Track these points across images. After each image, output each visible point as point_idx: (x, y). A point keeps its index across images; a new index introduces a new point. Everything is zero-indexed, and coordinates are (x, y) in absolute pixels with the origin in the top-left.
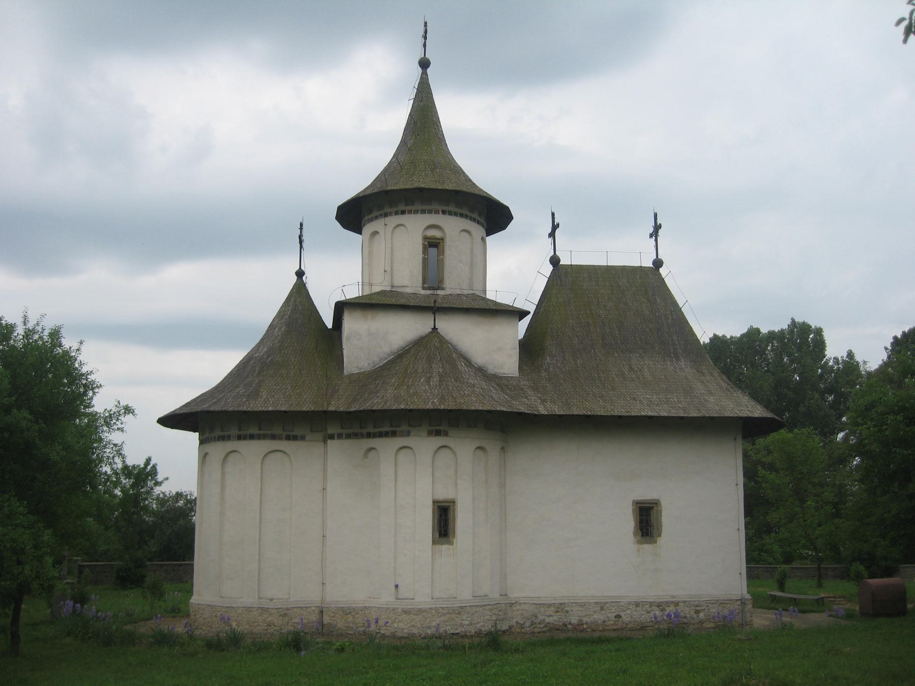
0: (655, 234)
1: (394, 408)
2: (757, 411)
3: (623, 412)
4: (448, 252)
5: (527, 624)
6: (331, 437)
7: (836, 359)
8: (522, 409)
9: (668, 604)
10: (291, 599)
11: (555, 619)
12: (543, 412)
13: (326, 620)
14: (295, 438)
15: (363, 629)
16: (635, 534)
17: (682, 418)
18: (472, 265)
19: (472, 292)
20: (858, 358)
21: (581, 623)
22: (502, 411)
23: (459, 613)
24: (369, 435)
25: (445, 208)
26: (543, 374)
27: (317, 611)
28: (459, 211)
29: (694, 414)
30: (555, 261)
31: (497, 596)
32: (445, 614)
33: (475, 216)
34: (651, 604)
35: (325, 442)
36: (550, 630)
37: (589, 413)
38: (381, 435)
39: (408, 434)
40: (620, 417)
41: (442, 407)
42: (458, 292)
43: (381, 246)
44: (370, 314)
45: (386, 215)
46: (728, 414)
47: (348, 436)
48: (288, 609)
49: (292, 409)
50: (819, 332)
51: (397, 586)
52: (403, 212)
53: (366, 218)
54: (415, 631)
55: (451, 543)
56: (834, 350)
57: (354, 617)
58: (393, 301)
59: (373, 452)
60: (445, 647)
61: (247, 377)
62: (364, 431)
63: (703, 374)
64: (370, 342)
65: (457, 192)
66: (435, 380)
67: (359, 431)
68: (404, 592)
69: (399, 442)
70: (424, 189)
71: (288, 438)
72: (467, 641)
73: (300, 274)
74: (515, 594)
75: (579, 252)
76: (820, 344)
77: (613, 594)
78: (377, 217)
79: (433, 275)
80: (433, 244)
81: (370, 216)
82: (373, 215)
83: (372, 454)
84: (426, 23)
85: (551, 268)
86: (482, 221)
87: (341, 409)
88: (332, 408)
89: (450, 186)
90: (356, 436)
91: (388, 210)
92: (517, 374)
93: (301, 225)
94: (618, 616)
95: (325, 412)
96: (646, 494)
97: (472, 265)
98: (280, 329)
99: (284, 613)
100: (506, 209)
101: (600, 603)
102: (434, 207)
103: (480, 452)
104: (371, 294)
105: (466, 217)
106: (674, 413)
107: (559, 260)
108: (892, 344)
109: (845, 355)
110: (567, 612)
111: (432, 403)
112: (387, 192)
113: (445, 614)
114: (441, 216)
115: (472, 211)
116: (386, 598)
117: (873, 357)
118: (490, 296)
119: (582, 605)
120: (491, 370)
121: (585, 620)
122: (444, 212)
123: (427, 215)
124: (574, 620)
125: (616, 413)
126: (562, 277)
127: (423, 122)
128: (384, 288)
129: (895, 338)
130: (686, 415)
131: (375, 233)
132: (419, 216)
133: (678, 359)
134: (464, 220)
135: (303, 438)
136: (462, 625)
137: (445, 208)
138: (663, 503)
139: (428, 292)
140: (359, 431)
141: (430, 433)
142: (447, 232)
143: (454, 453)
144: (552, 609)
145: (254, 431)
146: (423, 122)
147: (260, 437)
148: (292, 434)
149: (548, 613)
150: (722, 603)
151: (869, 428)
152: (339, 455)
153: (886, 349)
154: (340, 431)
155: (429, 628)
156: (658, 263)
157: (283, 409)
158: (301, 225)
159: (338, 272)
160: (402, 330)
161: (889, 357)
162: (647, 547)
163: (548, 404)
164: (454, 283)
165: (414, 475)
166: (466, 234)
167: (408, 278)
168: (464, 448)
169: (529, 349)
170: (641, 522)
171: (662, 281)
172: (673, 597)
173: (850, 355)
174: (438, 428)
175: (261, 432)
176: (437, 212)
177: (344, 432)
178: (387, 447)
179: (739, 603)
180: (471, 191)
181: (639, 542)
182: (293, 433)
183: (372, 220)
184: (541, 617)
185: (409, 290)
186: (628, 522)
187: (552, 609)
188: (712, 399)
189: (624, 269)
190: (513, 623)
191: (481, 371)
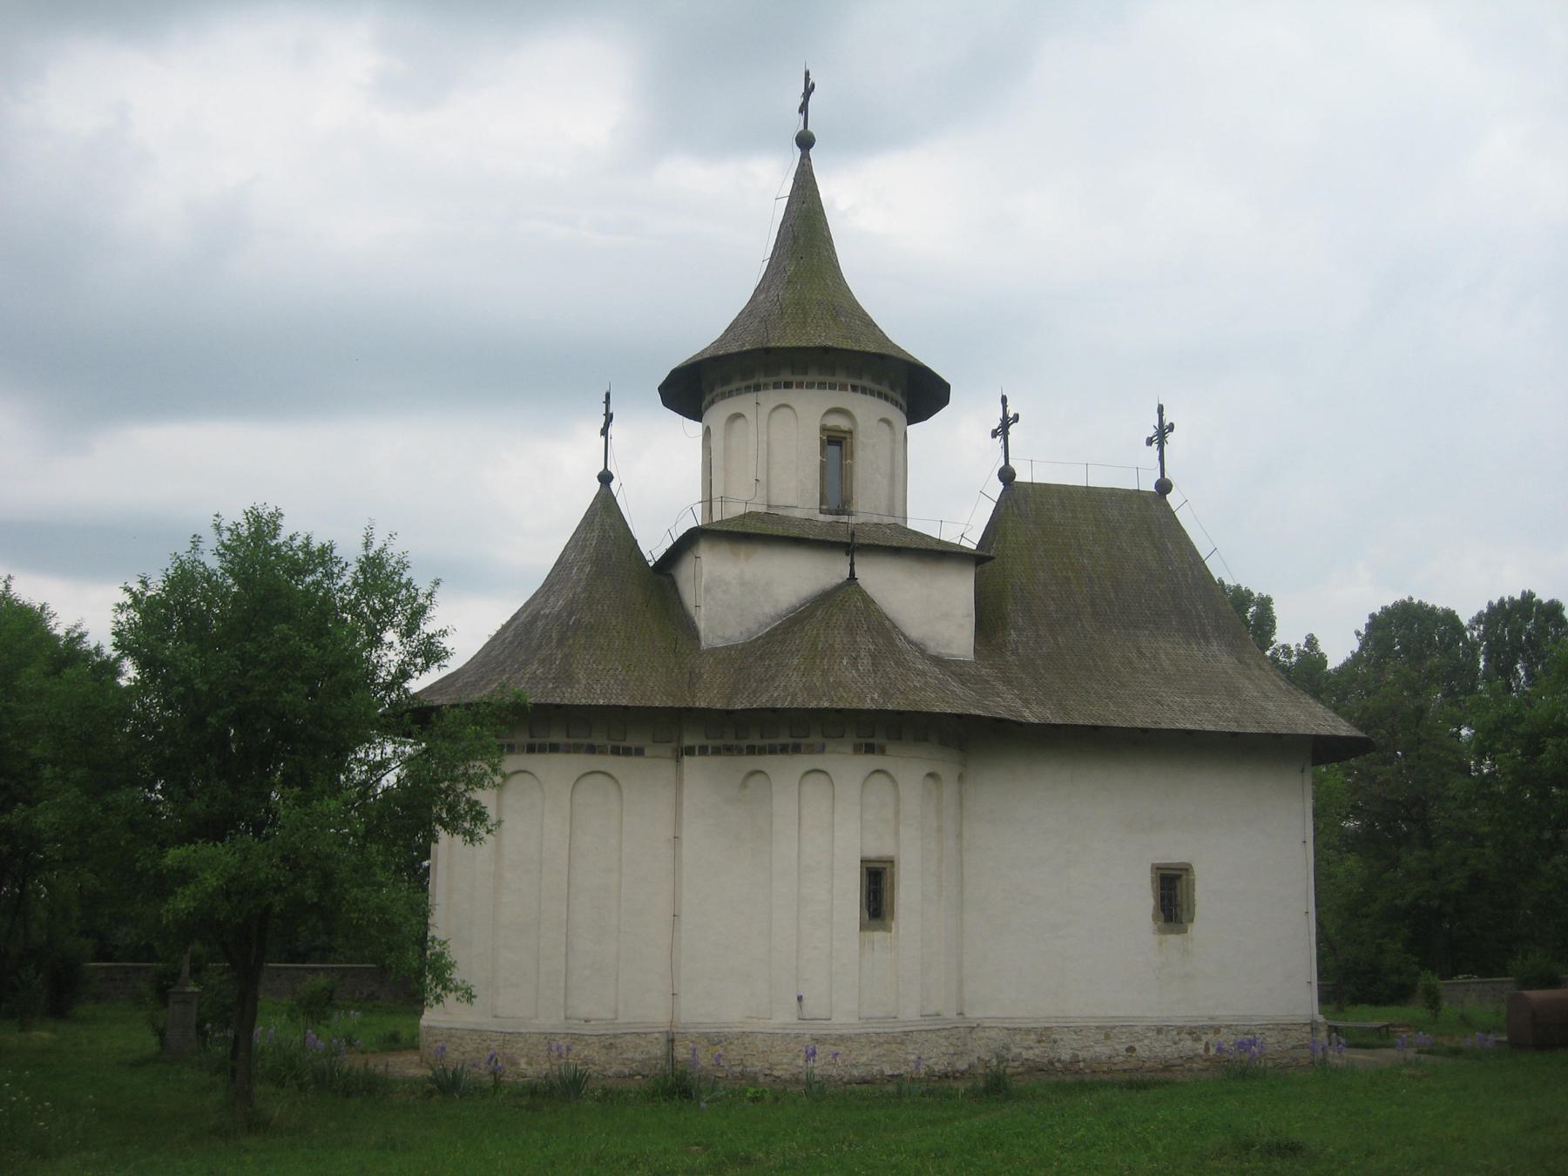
0: (1003, 430)
1: (813, 705)
2: (1344, 729)
3: (1148, 723)
5: (994, 1061)
6: (690, 751)
7: (1286, 650)
11: (1035, 1053)
13: (681, 1053)
14: (627, 752)
15: (739, 1069)
16: (1155, 918)
17: (1234, 735)
18: (892, 476)
19: (892, 520)
20: (1323, 647)
21: (1075, 1060)
22: (979, 716)
24: (751, 750)
25: (857, 382)
27: (663, 1039)
28: (877, 387)
29: (1252, 729)
30: (1006, 475)
32: (881, 1044)
34: (1180, 1030)
37: (1099, 723)
39: (822, 750)
40: (1145, 731)
42: (875, 520)
44: (743, 549)
45: (757, 388)
47: (717, 751)
48: (615, 1036)
49: (637, 704)
50: (1265, 603)
51: (800, 998)
52: (788, 385)
53: (718, 390)
54: (834, 1072)
55: (890, 930)
56: (1288, 634)
58: (779, 531)
59: (758, 778)
60: (930, 1092)
61: (539, 647)
62: (744, 743)
63: (1248, 665)
64: (738, 597)
65: (882, 357)
66: (865, 663)
68: (812, 1007)
69: (804, 762)
71: (616, 751)
72: (961, 1086)
73: (605, 478)
74: (975, 1014)
76: (1265, 623)
77: (1122, 1014)
78: (739, 391)
80: (836, 441)
81: (726, 389)
82: (734, 386)
84: (807, 74)
85: (1000, 486)
86: (904, 404)
87: (718, 706)
89: (872, 348)
90: (729, 750)
91: (762, 380)
92: (970, 657)
93: (608, 396)
94: (1131, 1049)
95: (690, 710)
97: (892, 476)
98: (581, 569)
99: (610, 1043)
100: (947, 387)
102: (840, 378)
103: (930, 782)
104: (744, 516)
105: (886, 398)
106: (1223, 726)
107: (1014, 475)
109: (1303, 642)
110: (1055, 1041)
111: (871, 701)
112: (768, 351)
113: (881, 1044)
115: (892, 388)
116: (783, 1018)
118: (912, 525)
120: (933, 649)
121: (1082, 1054)
122: (854, 389)
124: (1066, 1055)
126: (1019, 502)
129: (1372, 616)
133: (1208, 642)
134: (883, 402)
135: (640, 752)
136: (906, 1062)
137: (857, 382)
138: (1198, 869)
139: (830, 518)
140: (735, 742)
141: (857, 749)
144: (1033, 1036)
145: (558, 737)
147: (569, 749)
148: (622, 744)
149: (1026, 1044)
150: (1284, 1028)
151: (1514, 757)
152: (704, 781)
153: (1358, 633)
154: (705, 742)
155: (855, 1066)
156: (1164, 487)
157: (624, 702)
158: (608, 396)
159: (665, 477)
160: (794, 578)
161: (1361, 649)
162: (1174, 939)
164: (867, 508)
165: (830, 815)
166: (883, 425)
167: (795, 490)
168: (909, 770)
169: (989, 619)
170: (1162, 898)
171: (1171, 515)
172: (1212, 1019)
173: (1311, 641)
174: (870, 741)
175: (572, 741)
176: (843, 388)
177: (710, 743)
178: (785, 772)
179: (1308, 1029)
181: (1161, 931)
182: (626, 744)
184: (1016, 1050)
185: (798, 514)
186: (1145, 899)
187: (1033, 1036)
188: (1270, 706)
189: (1112, 492)
190: (973, 1059)
191: (920, 648)
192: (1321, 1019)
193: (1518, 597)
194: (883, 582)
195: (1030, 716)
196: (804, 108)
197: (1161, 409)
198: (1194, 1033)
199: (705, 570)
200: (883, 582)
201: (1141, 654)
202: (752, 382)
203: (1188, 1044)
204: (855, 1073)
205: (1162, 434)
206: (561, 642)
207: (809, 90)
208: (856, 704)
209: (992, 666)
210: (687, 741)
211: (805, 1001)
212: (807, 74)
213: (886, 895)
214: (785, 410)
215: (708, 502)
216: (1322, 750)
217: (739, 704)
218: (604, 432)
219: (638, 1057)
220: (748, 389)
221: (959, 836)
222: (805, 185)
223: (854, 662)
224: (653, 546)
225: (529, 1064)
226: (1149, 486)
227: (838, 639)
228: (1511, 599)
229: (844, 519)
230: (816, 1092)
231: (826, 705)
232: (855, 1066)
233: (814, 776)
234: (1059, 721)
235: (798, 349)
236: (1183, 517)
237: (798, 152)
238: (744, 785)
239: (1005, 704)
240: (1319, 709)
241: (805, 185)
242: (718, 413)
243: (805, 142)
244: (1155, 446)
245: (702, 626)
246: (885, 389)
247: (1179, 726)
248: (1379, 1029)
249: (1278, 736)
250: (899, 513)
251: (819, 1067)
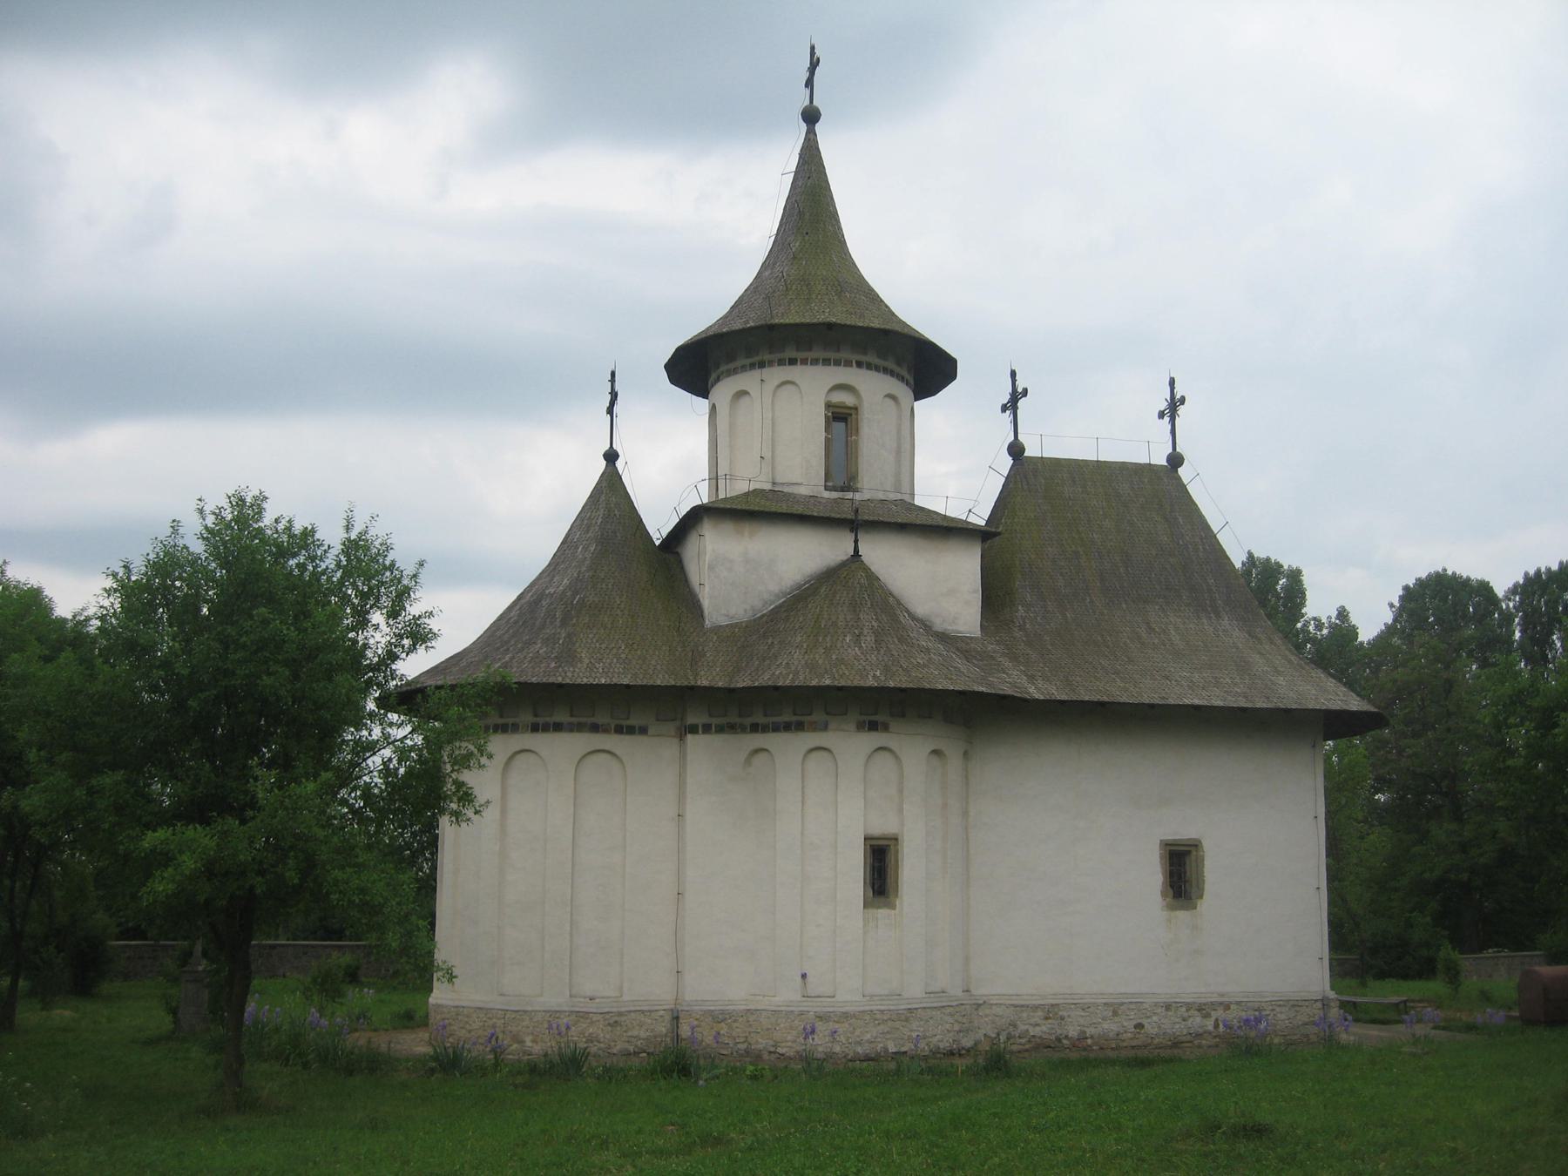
1: (814, 683)
2: (1355, 704)
4: (865, 430)
6: (693, 730)
8: (1007, 690)
9: (1213, 1005)
10: (626, 998)
11: (1042, 1030)
12: (1037, 696)
14: (631, 730)
15: (743, 1046)
16: (1164, 895)
18: (899, 452)
19: (899, 497)
20: (1354, 619)
21: (1083, 1037)
23: (907, 1020)
24: (755, 728)
26: (1018, 634)
27: (668, 1017)
30: (1016, 450)
31: (959, 993)
32: (885, 1021)
33: (904, 373)
34: (1189, 1006)
35: (682, 737)
36: (1037, 1047)
37: (1105, 699)
38: (776, 728)
39: (825, 728)
40: (1152, 706)
41: (892, 684)
42: (881, 496)
43: (754, 413)
44: (747, 527)
45: (762, 365)
46: (1312, 705)
47: (720, 729)
48: (620, 1014)
50: (1295, 576)
51: (804, 976)
52: (792, 362)
53: (723, 368)
55: (893, 907)
56: (1318, 607)
57: (730, 1027)
58: (783, 508)
59: (762, 757)
60: (930, 1070)
61: (543, 627)
62: (748, 721)
64: (742, 575)
65: (886, 332)
66: (868, 640)
67: (738, 720)
70: (811, 324)
71: (619, 730)
72: (961, 1064)
73: (611, 456)
74: (981, 991)
75: (1051, 438)
76: (1296, 593)
78: (744, 369)
79: (842, 464)
80: (841, 417)
82: (738, 363)
83: (759, 760)
84: (813, 48)
85: (1009, 461)
87: (720, 684)
88: (704, 682)
89: (876, 324)
90: (732, 728)
91: (767, 357)
92: (977, 633)
93: (613, 374)
94: (1140, 1026)
95: (692, 688)
96: (1181, 829)
97: (899, 452)
98: (586, 549)
99: (615, 1021)
101: (1112, 1004)
102: (844, 354)
104: (747, 494)
106: (1232, 702)
108: (1402, 598)
109: (1334, 614)
110: (1062, 1018)
112: (772, 327)
113: (885, 1021)
114: (854, 370)
115: (899, 364)
116: (787, 995)
117: (1372, 620)
118: (918, 502)
119: (1085, 1008)
120: (939, 625)
121: (1090, 1031)
122: (859, 365)
123: (832, 369)
124: (1073, 1032)
125: (1146, 700)
126: (1028, 476)
127: (810, 209)
128: (758, 486)
129: (1406, 588)
130: (1249, 705)
131: (742, 393)
132: (819, 370)
133: (1218, 616)
135: (643, 731)
138: (1206, 844)
139: (835, 495)
140: (738, 720)
141: (861, 727)
142: (863, 394)
143: (897, 757)
144: (1040, 1013)
145: (562, 717)
146: (810, 209)
148: (625, 723)
150: (1295, 1005)
153: (1391, 605)
155: (859, 1043)
156: (1176, 460)
157: (625, 681)
158: (613, 374)
160: (798, 556)
161: (1395, 620)
162: (1182, 915)
163: (1040, 683)
164: (873, 485)
165: (833, 794)
166: (890, 402)
167: (801, 468)
168: (914, 750)
169: (996, 595)
170: (1171, 874)
172: (1222, 995)
173: (1343, 614)
176: (848, 364)
177: (714, 721)
178: (788, 749)
179: (1319, 1005)
180: (897, 328)
181: (1171, 908)
182: (629, 722)
183: (735, 371)
184: (1022, 1027)
185: (803, 491)
186: (1154, 875)
187: (1040, 1013)
189: (1123, 466)
190: (980, 1035)
191: (925, 625)
192: (1332, 995)
193: (1555, 567)
194: (891, 561)
195: (1035, 691)
196: (809, 83)
197: (1172, 382)
198: (1203, 1009)
199: (709, 548)
200: (891, 561)
201: (1150, 629)
202: (756, 359)
203: (1196, 1021)
204: (859, 1050)
205: (1174, 405)
206: (564, 623)
207: (814, 64)
208: (857, 682)
209: (998, 643)
210: (691, 720)
211: (810, 979)
212: (813, 48)
213: (890, 872)
214: (789, 387)
215: (714, 479)
216: (1336, 724)
217: (741, 683)
218: (610, 411)
219: (643, 1034)
220: (752, 366)
221: (965, 813)
222: (810, 160)
223: (858, 639)
224: (659, 525)
225: (534, 1041)
226: (1160, 460)
227: (841, 617)
228: (1549, 570)
229: (849, 495)
230: (814, 1068)
231: (828, 682)
232: (859, 1043)
233: (814, 755)
234: (1064, 697)
235: (802, 325)
236: (1195, 491)
237: (804, 127)
238: (748, 762)
239: (1012, 680)
240: (1331, 683)
241: (810, 160)
242: (723, 391)
243: (811, 116)
244: (1167, 419)
245: (706, 603)
246: (891, 365)
247: (1187, 702)
248: (1397, 1005)
249: (1287, 711)
250: (905, 488)
251: (820, 1043)
